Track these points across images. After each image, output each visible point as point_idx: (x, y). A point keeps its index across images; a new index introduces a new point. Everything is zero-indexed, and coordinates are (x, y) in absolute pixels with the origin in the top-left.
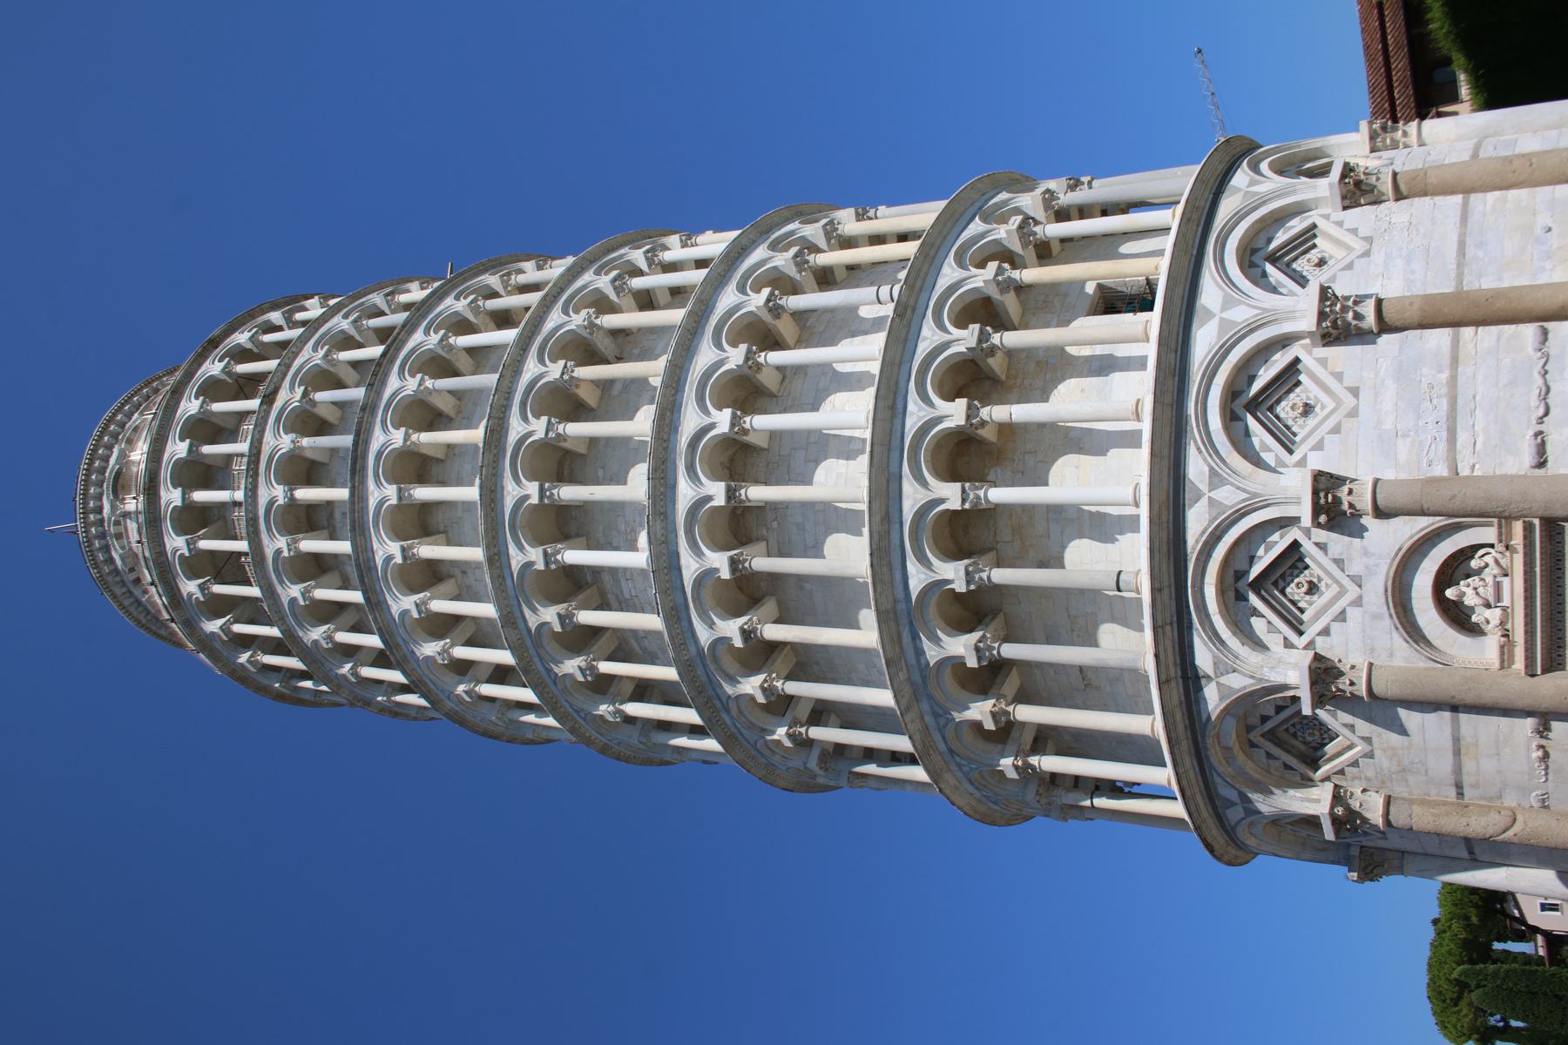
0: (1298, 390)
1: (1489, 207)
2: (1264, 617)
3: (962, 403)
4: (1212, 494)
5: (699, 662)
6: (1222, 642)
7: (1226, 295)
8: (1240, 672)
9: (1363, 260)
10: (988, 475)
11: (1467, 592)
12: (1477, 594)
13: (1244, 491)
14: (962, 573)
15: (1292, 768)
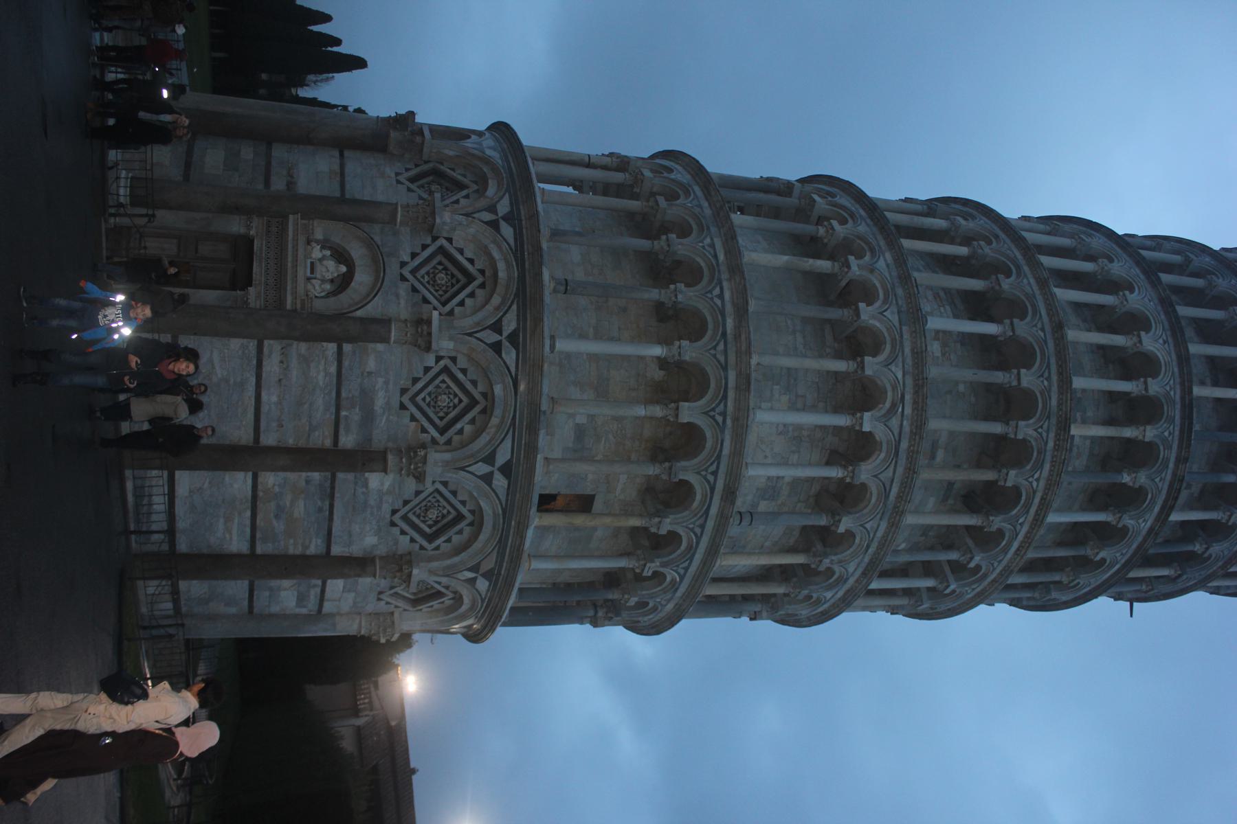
0: (441, 414)
1: (314, 540)
2: (466, 258)
3: (685, 418)
4: (500, 338)
5: (883, 248)
6: (494, 242)
7: (489, 483)
8: (483, 222)
9: (397, 508)
10: (665, 376)
11: (332, 269)
12: (327, 268)
13: (478, 339)
14: (680, 297)
15: (450, 169)
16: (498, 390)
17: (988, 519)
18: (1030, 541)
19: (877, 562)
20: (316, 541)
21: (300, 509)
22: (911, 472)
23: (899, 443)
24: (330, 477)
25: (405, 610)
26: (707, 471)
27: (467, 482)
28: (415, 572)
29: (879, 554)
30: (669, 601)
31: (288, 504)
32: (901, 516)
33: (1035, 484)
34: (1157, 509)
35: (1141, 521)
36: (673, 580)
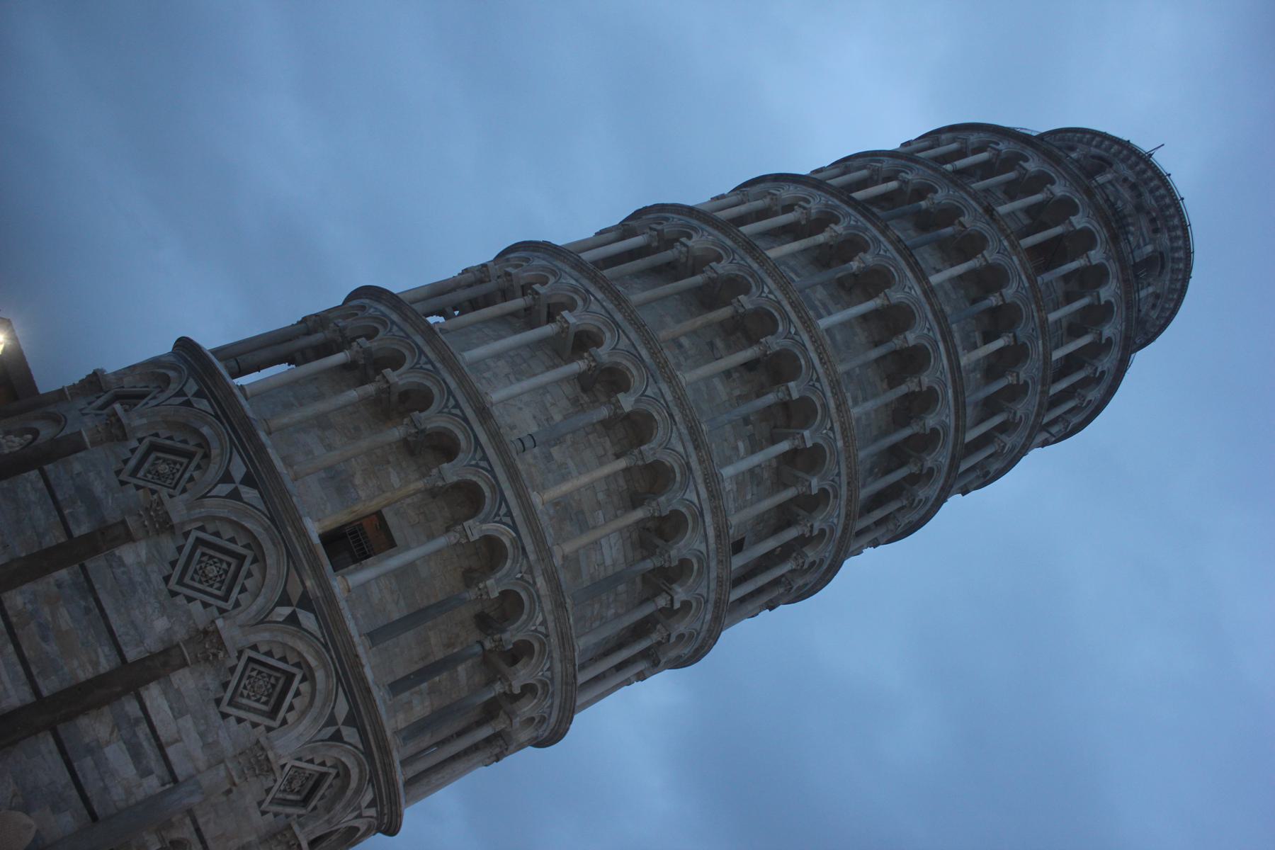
1: (99, 650)
9: (166, 573)
16: (205, 430)
17: (761, 343)
18: (819, 342)
19: (693, 424)
20: (103, 651)
21: (65, 619)
22: (642, 328)
23: (614, 319)
24: (80, 571)
25: (269, 729)
26: (447, 407)
27: (213, 507)
28: (220, 623)
29: (687, 416)
30: (530, 570)
31: (50, 619)
32: (667, 366)
33: (771, 296)
34: (910, 274)
35: (907, 290)
36: (513, 541)
